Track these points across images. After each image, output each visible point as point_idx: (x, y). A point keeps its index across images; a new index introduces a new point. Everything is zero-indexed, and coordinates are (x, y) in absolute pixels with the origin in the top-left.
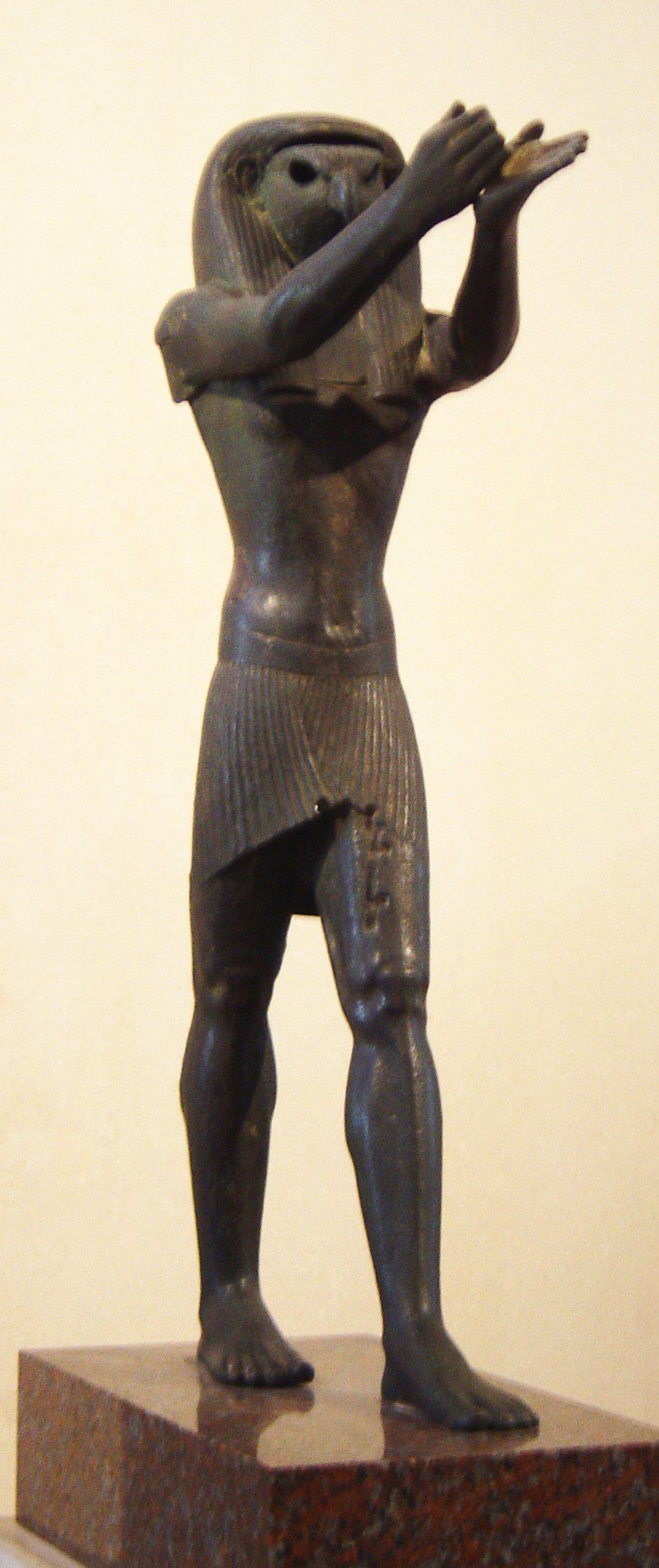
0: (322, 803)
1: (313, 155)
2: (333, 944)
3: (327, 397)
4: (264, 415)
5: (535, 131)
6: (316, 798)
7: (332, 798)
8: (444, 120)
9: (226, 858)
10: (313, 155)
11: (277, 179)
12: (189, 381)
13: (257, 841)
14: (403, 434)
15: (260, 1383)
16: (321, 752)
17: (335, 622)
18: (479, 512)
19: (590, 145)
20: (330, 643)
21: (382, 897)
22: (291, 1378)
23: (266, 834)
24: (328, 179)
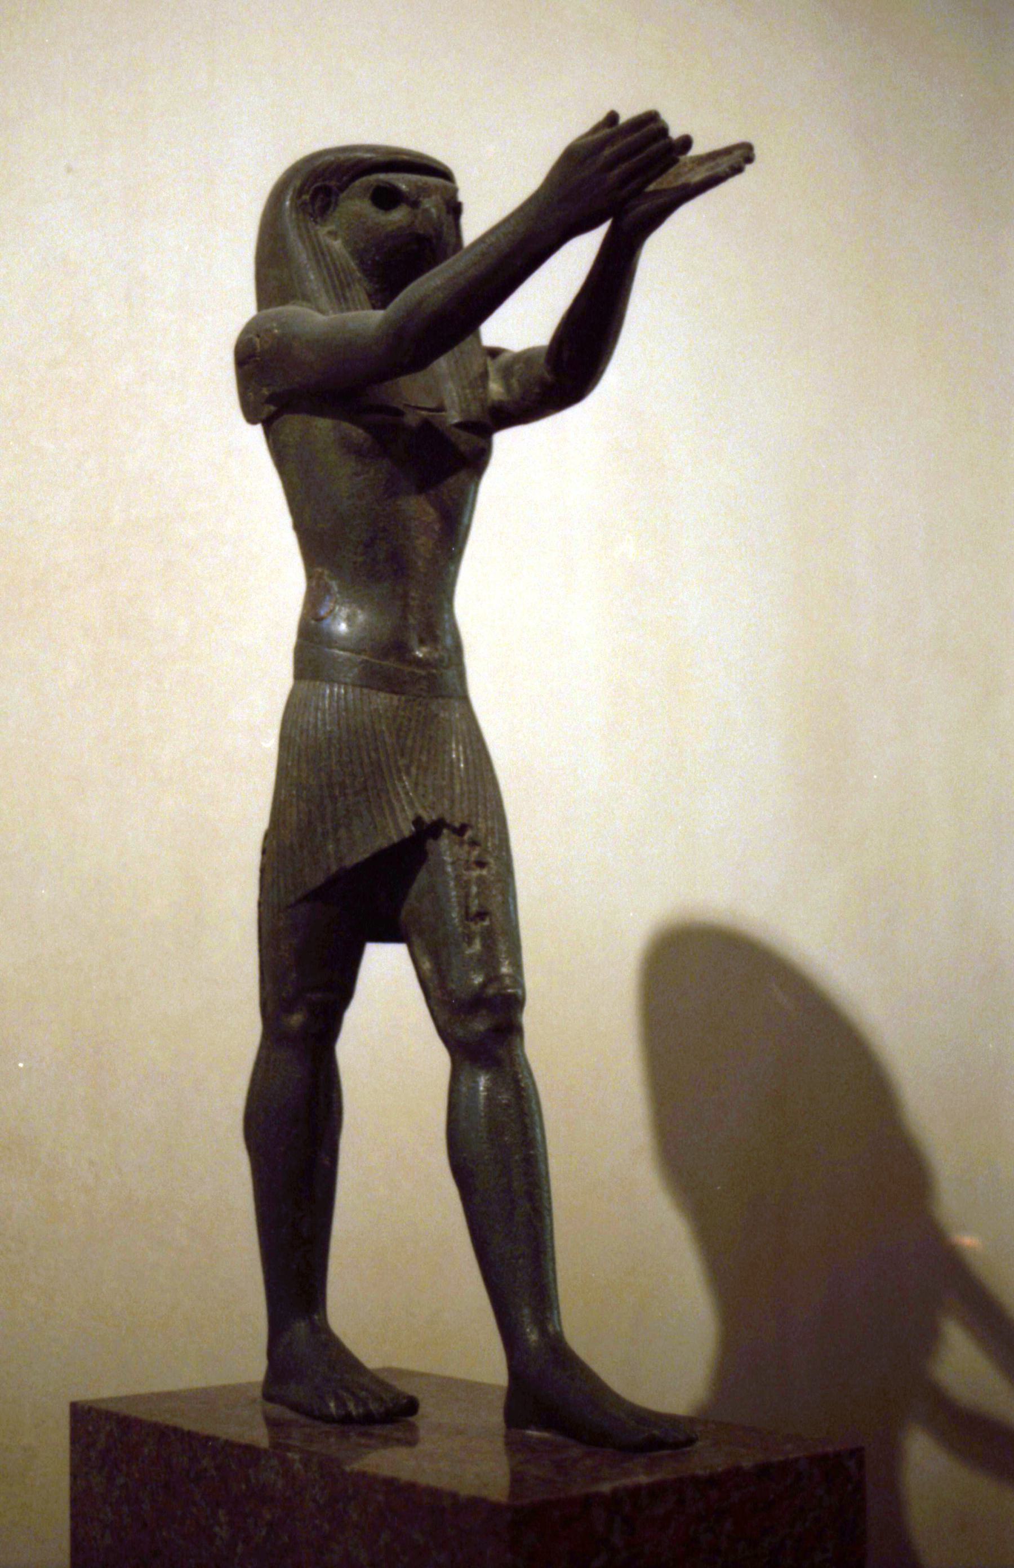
0: (418, 821)
1: (403, 182)
2: (427, 966)
3: (411, 419)
4: (357, 433)
5: (686, 143)
6: (410, 815)
7: (429, 817)
8: (596, 129)
9: (316, 879)
10: (403, 182)
11: (356, 205)
12: (270, 400)
13: (350, 861)
14: (477, 461)
15: (369, 1419)
16: (414, 770)
17: (422, 642)
18: (546, 540)
19: (757, 152)
20: (419, 662)
21: (482, 915)
22: (391, 1409)
23: (360, 854)
24: (415, 204)
